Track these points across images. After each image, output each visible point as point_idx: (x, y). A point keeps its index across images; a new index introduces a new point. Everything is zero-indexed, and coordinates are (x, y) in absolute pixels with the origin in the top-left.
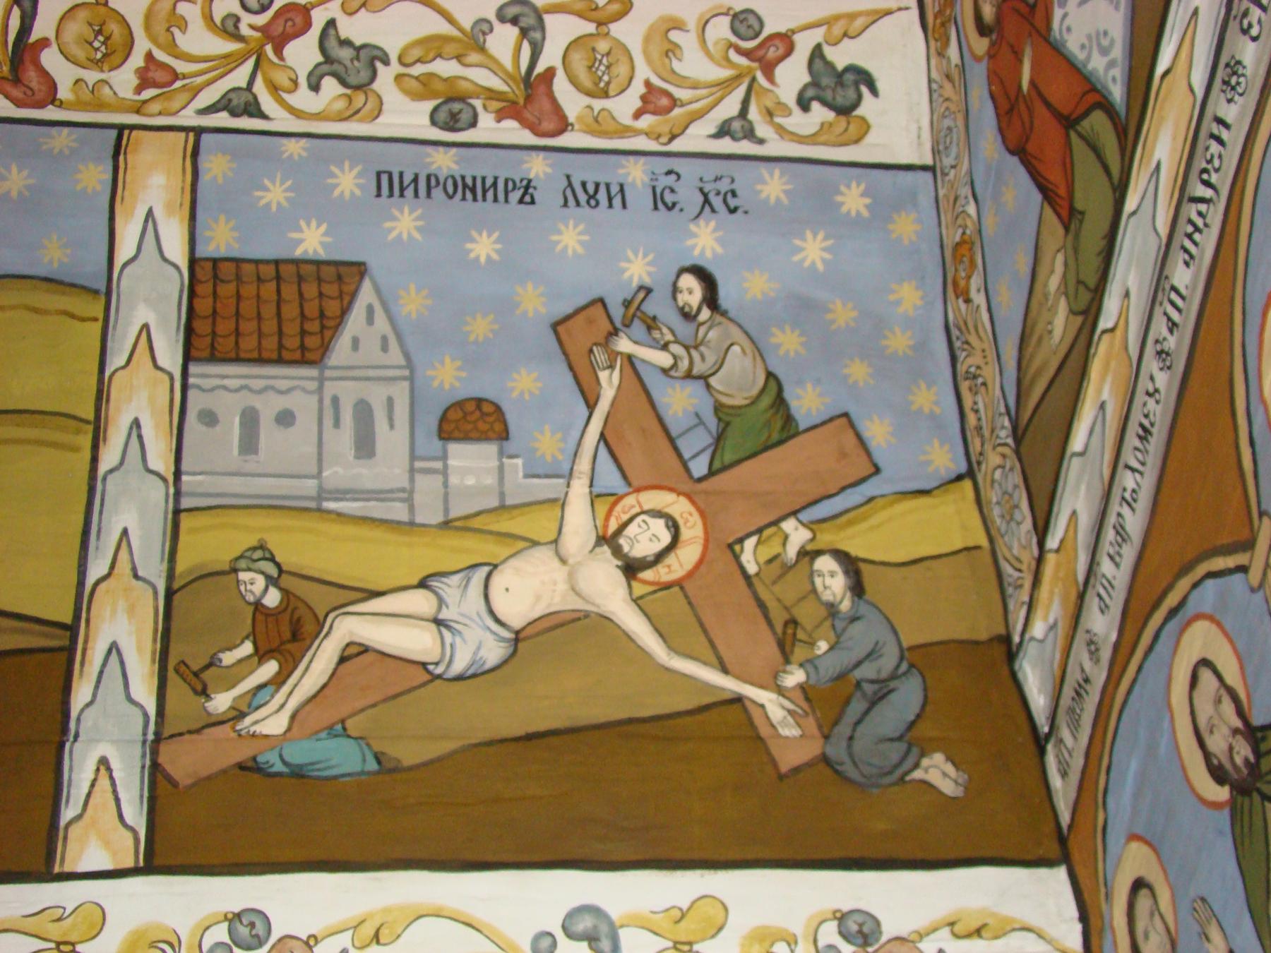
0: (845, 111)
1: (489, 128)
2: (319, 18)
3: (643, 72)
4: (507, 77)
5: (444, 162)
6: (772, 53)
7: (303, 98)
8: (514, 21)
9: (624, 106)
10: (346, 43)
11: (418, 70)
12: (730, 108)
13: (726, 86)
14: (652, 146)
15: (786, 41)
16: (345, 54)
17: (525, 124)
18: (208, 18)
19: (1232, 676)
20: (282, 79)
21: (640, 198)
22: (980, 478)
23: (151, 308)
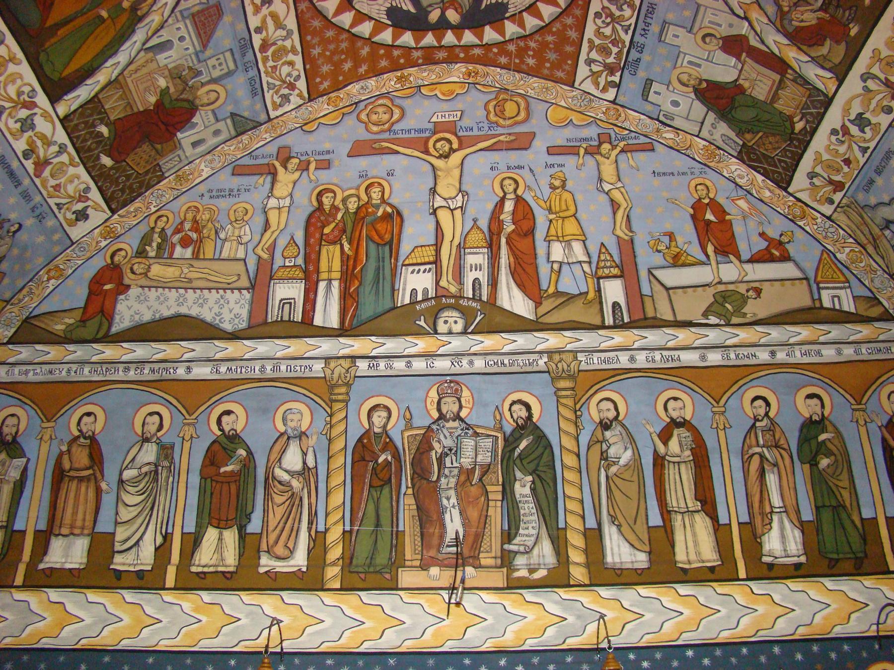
0: (77, 220)
1: (29, 165)
2: (36, 110)
3: (63, 180)
4: (45, 156)
5: (15, 164)
6: (83, 199)
7: (11, 123)
8: (60, 148)
9: (52, 182)
10: (32, 120)
11: (35, 139)
12: (63, 201)
13: (70, 197)
14: (45, 196)
15: (88, 199)
16: (29, 122)
17: (35, 169)
18: (20, 87)
19: (22, 427)
20: (14, 114)
21: (32, 204)
22: (9, 307)
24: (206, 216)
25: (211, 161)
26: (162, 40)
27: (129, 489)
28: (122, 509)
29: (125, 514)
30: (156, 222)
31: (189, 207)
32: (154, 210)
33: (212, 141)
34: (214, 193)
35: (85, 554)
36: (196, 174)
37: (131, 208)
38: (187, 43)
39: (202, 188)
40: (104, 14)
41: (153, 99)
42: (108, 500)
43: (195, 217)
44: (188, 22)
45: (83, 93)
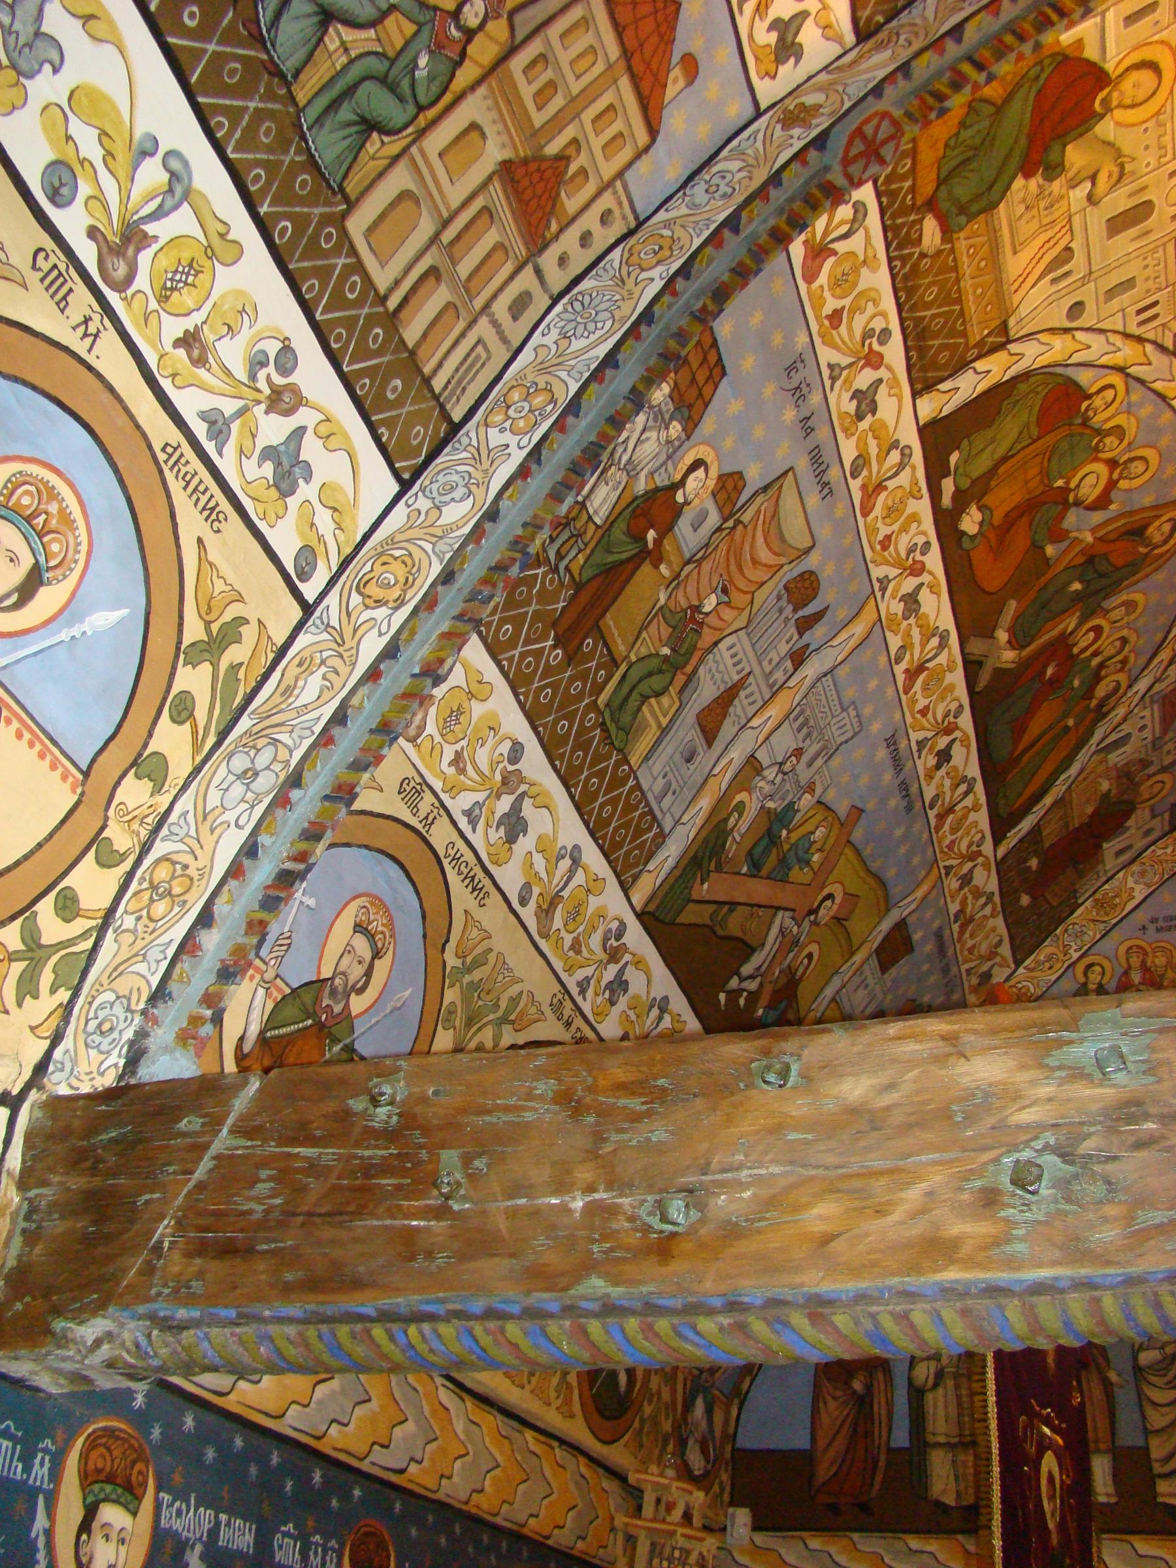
1: (956, 927)
23: (885, 926)
24: (1161, 960)
25: (1142, 874)
26: (1122, 734)
27: (1153, 1379)
28: (1149, 1411)
29: (1157, 1419)
30: (1085, 974)
31: (1131, 948)
32: (1076, 956)
33: (1139, 845)
34: (1161, 923)
35: (1110, 1482)
36: (1125, 896)
37: (1042, 954)
38: (1147, 733)
39: (1141, 916)
40: (1071, 722)
41: (1089, 810)
42: (1125, 1397)
43: (1143, 963)
44: (1156, 707)
45: (1026, 825)
